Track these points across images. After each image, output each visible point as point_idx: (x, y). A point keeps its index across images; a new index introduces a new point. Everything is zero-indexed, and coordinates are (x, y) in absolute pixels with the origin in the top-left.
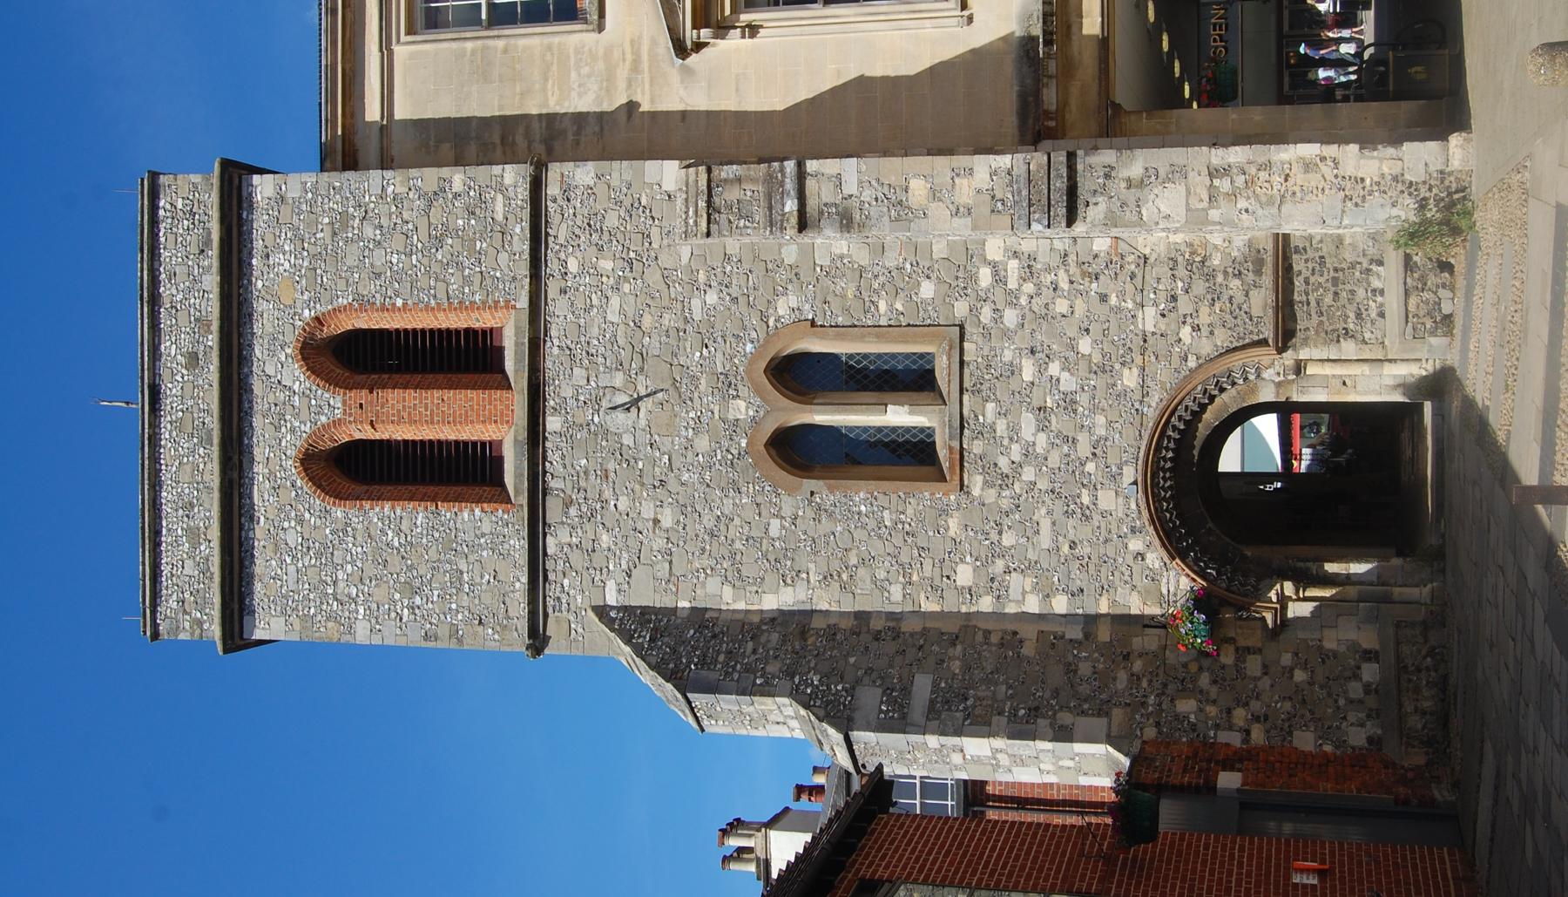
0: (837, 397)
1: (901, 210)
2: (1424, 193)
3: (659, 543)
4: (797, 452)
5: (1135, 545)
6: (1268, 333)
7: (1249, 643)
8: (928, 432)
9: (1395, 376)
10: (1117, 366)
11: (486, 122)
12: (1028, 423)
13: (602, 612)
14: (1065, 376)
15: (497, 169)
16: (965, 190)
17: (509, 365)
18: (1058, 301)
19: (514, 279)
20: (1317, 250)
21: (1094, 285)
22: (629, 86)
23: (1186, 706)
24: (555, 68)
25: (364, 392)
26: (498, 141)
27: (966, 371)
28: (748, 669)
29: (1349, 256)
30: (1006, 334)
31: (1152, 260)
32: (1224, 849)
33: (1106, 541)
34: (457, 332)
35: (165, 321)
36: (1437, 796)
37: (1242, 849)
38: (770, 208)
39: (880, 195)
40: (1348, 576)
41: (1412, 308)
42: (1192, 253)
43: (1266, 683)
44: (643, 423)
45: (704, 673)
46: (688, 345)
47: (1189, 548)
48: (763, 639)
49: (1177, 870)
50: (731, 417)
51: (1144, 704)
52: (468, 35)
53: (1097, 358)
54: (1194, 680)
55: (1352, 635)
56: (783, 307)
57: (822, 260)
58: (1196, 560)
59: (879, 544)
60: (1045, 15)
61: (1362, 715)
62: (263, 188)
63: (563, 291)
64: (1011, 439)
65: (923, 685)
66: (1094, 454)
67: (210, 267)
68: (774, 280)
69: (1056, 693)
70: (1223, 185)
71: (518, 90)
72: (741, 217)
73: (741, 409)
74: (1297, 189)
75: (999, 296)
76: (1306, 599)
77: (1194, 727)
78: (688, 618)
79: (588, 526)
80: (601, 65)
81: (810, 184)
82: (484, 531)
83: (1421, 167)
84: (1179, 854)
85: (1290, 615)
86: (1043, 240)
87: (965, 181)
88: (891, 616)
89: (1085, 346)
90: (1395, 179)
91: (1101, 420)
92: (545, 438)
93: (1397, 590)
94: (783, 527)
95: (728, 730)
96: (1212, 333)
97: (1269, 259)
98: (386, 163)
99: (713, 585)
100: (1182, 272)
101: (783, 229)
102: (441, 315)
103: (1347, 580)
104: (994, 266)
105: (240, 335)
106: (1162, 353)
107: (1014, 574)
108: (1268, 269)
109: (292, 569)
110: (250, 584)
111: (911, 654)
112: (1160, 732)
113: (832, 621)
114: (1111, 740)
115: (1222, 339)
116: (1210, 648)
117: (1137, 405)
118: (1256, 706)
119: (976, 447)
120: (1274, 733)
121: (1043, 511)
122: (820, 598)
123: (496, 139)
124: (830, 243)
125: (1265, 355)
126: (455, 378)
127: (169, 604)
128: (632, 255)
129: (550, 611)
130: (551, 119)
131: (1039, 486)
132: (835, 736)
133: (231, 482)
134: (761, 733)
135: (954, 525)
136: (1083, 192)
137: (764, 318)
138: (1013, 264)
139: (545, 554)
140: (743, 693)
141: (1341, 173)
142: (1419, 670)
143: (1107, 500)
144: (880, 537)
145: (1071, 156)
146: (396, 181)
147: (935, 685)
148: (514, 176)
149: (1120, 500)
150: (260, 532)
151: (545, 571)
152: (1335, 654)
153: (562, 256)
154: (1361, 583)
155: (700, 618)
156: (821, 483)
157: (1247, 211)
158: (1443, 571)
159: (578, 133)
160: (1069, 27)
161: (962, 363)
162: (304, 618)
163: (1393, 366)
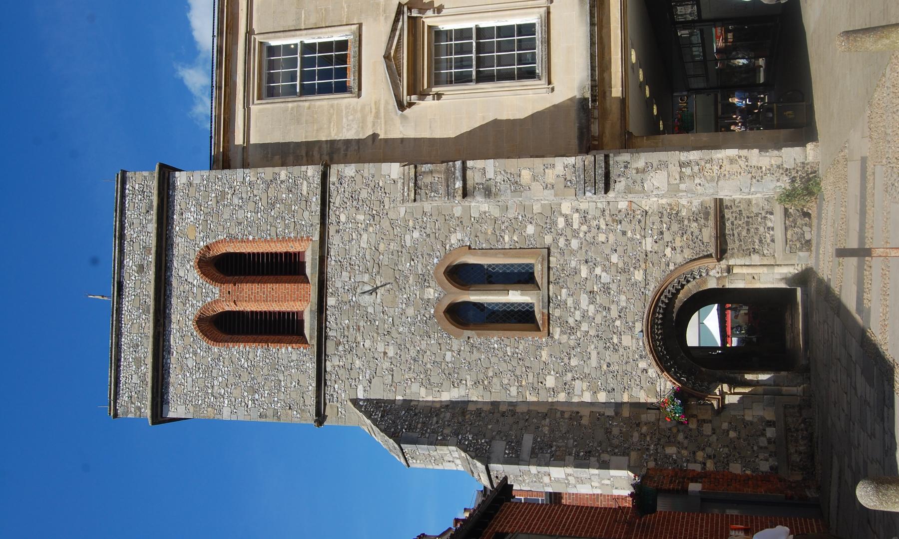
0: (482, 287)
1: (517, 186)
2: (794, 174)
3: (386, 365)
4: (460, 316)
5: (642, 364)
6: (712, 250)
7: (705, 417)
8: (531, 306)
9: (781, 274)
10: (632, 269)
11: (298, 145)
12: (584, 299)
13: (355, 402)
14: (604, 274)
15: (304, 168)
16: (550, 176)
17: (308, 271)
18: (600, 235)
19: (312, 225)
20: (738, 207)
21: (619, 226)
22: (374, 125)
23: (671, 450)
24: (335, 116)
25: (231, 285)
26: (304, 154)
27: (551, 272)
28: (434, 432)
29: (755, 210)
30: (573, 253)
31: (650, 213)
32: (693, 519)
33: (627, 363)
34: (281, 254)
35: (127, 248)
36: (808, 493)
37: (702, 519)
38: (448, 186)
39: (506, 179)
40: (758, 381)
41: (789, 237)
42: (671, 209)
43: (714, 437)
44: (379, 301)
45: (410, 434)
47: (671, 366)
48: (442, 416)
49: (667, 529)
50: (426, 297)
51: (648, 449)
52: (290, 100)
53: (621, 265)
54: (675, 437)
55: (761, 413)
56: (454, 239)
57: (475, 214)
58: (675, 373)
59: (504, 365)
60: (592, 87)
61: (767, 455)
62: (181, 178)
64: (575, 308)
65: (528, 440)
67: (152, 219)
70: (687, 171)
71: (315, 128)
73: (431, 293)
74: (726, 173)
75: (569, 232)
76: (735, 394)
77: (675, 462)
78: (402, 405)
79: (348, 356)
80: (359, 115)
81: (469, 173)
82: (293, 360)
83: (792, 161)
84: (668, 521)
85: (727, 402)
86: (592, 202)
87: (550, 171)
88: (511, 404)
89: (614, 258)
90: (778, 167)
91: (623, 298)
92: (326, 309)
93: (784, 389)
94: (453, 356)
95: (422, 466)
96: (682, 251)
97: (712, 212)
98: (245, 165)
99: (415, 387)
100: (665, 219)
101: (454, 197)
102: (273, 244)
103: (757, 383)
105: (166, 255)
106: (655, 262)
108: (712, 217)
109: (190, 379)
110: (167, 387)
111: (522, 424)
112: (657, 464)
113: (479, 407)
114: (630, 468)
115: (688, 254)
116: (683, 420)
117: (642, 290)
118: (709, 450)
119: (557, 313)
120: (719, 464)
121: (593, 347)
122: (472, 394)
123: (303, 153)
124: (479, 205)
125: (711, 263)
126: (279, 278)
127: (124, 398)
128: (374, 212)
129: (327, 401)
130: (332, 142)
131: (590, 333)
132: (480, 466)
133: (159, 333)
134: (440, 467)
135: (545, 354)
136: (613, 176)
137: (443, 245)
138: (576, 216)
139: (325, 371)
140: (431, 444)
141: (749, 164)
142: (797, 430)
143: (627, 340)
144: (505, 361)
145: (607, 157)
146: (250, 175)
147: (535, 439)
148: (312, 172)
149: (634, 341)
150: (173, 361)
151: (325, 380)
152: (752, 423)
153: (337, 213)
154: (765, 385)
155: (407, 404)
156: (473, 332)
158: (809, 378)
159: (347, 150)
160: (605, 93)
161: (549, 268)
162: (196, 406)
163: (779, 268)
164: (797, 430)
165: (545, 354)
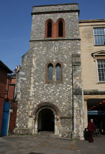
3: (41, 53)
5: (39, 102)
12: (53, 90)
14: (58, 94)
24: (90, 42)
30: (62, 88)
54: (25, 108)
56: (65, 64)
61: (20, 125)
62: (77, 14)
63: (67, 43)
69: (23, 93)
70: (78, 111)
73: (54, 60)
77: (19, 107)
82: (43, 36)
89: (61, 96)
90: (79, 131)
91: (53, 98)
100: (69, 107)
104: (70, 87)
135: (42, 83)
165: (42, 83)
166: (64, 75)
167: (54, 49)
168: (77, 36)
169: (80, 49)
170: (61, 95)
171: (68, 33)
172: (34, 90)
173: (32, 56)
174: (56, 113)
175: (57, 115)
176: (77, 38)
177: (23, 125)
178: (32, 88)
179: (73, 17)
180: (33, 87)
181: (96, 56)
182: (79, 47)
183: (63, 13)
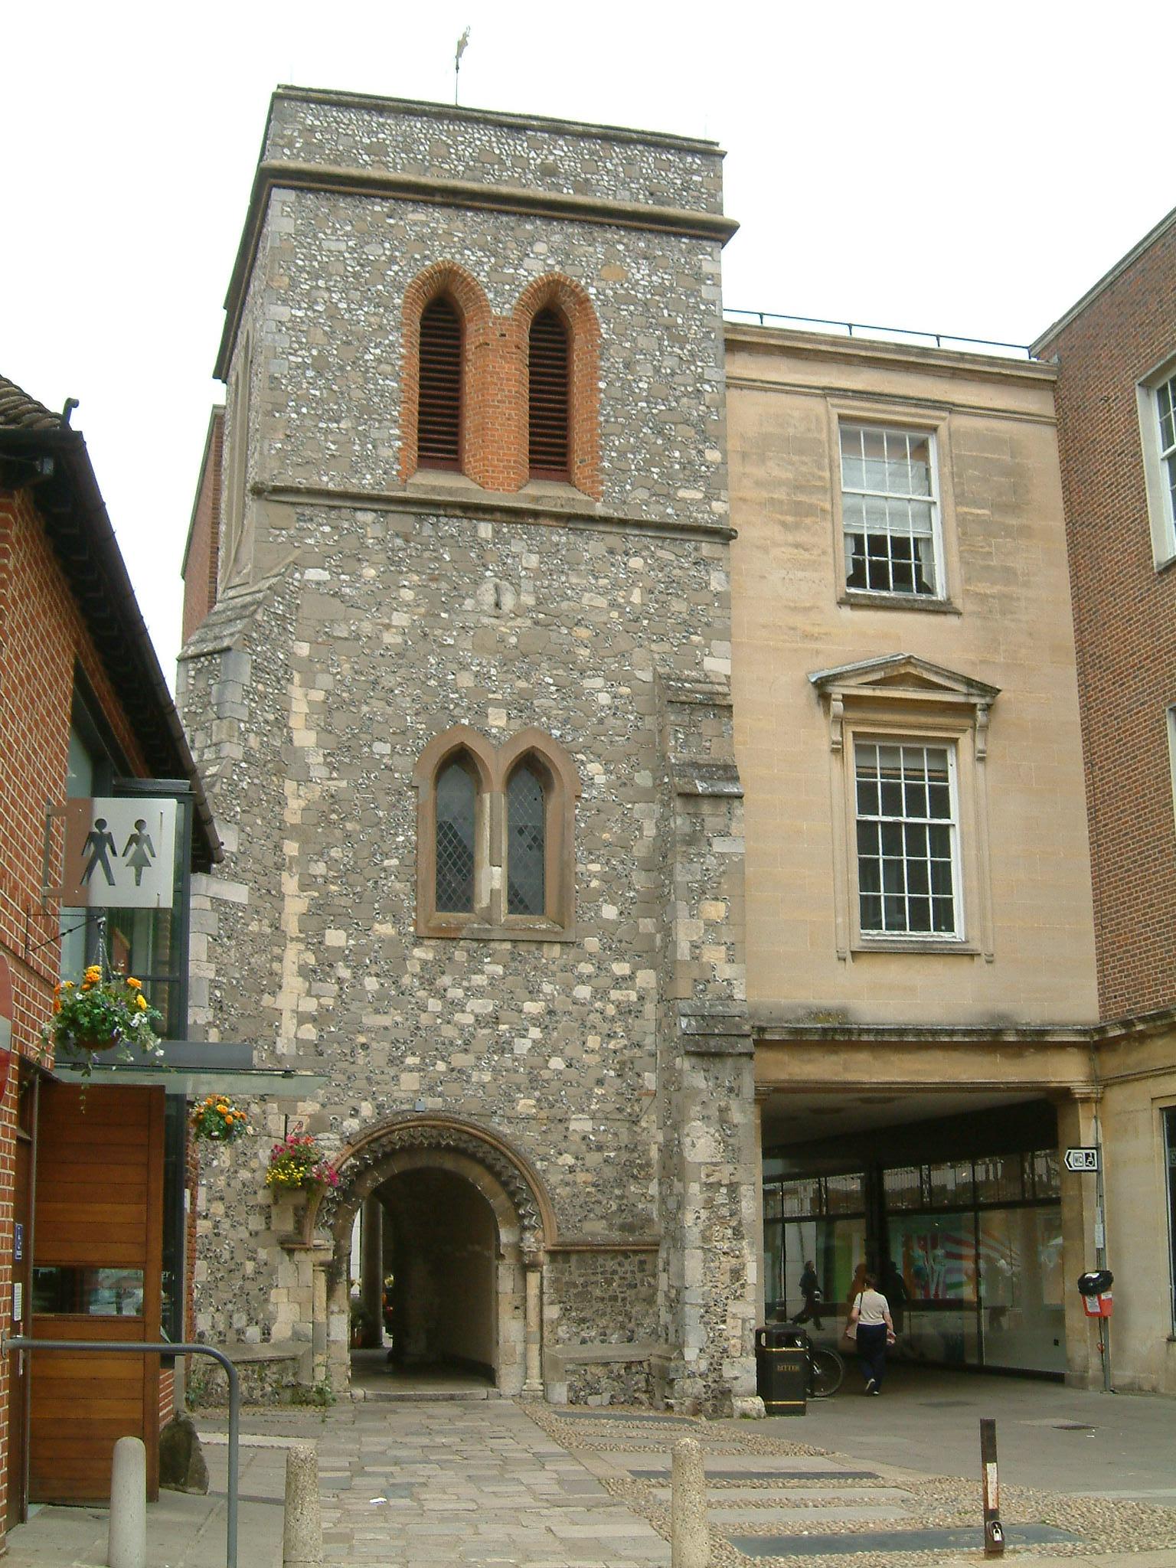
5: (367, 1109)
12: (483, 1006)
14: (528, 1043)
20: (642, 1281)
21: (612, 1073)
24: (807, 555)
26: (740, 495)
27: (533, 947)
44: (485, 620)
46: (561, 672)
50: (490, 710)
54: (245, 1165)
56: (594, 768)
61: (221, 1327)
63: (611, 552)
64: (468, 989)
66: (453, 1070)
68: (620, 762)
70: (721, 1196)
72: (687, 735)
73: (497, 720)
75: (604, 981)
77: (208, 1164)
79: (382, 556)
87: (723, 955)
89: (557, 1063)
90: (725, 1351)
91: (487, 1077)
92: (470, 519)
94: (382, 756)
96: (567, 1184)
100: (625, 1156)
104: (632, 977)
107: (336, 987)
109: (343, 247)
118: (226, 1224)
119: (460, 956)
121: (399, 1019)
131: (423, 1016)
135: (385, 929)
137: (585, 749)
139: (356, 509)
143: (410, 1082)
152: (267, 1300)
157: (698, 1218)
164: (262, 1379)
165: (385, 929)
166: (580, 868)
167: (497, 605)
168: (709, 498)
169: (728, 629)
170: (556, 1051)
171: (622, 455)
172: (309, 994)
173: (290, 654)
174: (518, 1205)
175: (524, 1229)
176: (702, 518)
177: (240, 1320)
178: (292, 983)
179: (672, 289)
180: (304, 972)
181: (849, 701)
182: (715, 611)
183: (577, 230)
